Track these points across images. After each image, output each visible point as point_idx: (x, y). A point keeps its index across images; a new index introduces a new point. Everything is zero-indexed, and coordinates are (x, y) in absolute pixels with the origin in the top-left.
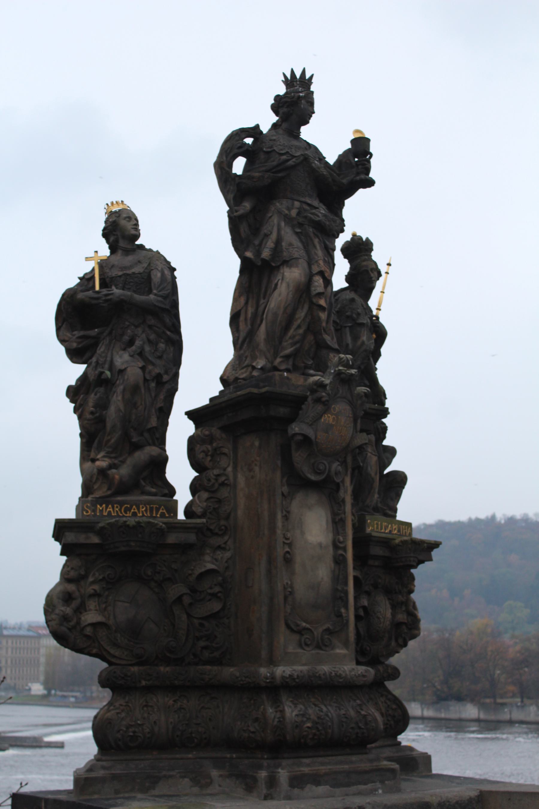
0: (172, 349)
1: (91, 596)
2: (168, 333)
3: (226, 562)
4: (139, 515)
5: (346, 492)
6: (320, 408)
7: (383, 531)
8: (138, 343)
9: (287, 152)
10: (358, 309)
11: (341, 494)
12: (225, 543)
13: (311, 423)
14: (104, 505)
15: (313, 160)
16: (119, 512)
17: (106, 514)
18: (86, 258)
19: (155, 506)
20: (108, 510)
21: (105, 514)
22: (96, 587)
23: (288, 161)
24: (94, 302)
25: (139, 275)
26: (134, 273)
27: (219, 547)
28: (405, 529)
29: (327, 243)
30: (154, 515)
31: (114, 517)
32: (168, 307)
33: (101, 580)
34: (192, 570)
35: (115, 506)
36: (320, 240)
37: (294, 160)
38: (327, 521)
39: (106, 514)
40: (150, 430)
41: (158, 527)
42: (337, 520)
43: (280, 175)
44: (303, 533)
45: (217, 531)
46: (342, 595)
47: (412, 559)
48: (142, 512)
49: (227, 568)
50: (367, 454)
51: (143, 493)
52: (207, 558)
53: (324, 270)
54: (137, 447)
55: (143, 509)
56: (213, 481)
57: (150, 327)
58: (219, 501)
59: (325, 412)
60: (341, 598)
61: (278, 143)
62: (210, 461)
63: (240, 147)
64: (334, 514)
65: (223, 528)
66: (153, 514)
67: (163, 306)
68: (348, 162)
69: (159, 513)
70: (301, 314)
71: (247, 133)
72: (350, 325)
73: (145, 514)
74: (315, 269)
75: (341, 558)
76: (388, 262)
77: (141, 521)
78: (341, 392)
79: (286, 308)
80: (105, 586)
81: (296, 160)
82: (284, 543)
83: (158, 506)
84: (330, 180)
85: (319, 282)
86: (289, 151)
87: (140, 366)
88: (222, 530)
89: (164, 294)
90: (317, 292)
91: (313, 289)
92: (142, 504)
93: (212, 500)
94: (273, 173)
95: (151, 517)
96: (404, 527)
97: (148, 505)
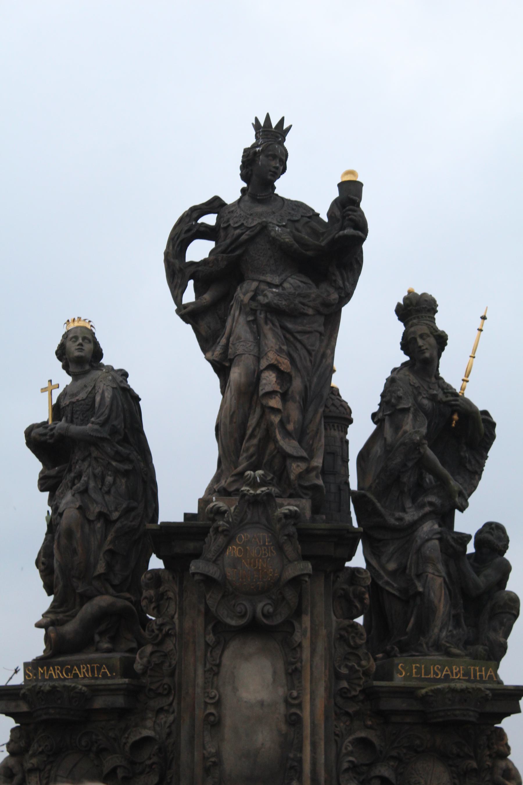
0: (123, 481)
1: (31, 771)
2: (114, 463)
3: (169, 727)
4: (80, 676)
5: (304, 634)
6: (221, 540)
7: (432, 676)
8: (84, 479)
9: (242, 224)
10: (399, 390)
11: (297, 637)
12: (171, 704)
13: (214, 558)
14: (45, 668)
15: (273, 227)
16: (60, 675)
17: (48, 678)
18: (42, 389)
19: (95, 665)
20: (50, 672)
21: (47, 677)
22: (34, 761)
23: (242, 234)
24: (43, 439)
25: (83, 402)
26: (78, 401)
27: (161, 710)
28: (480, 671)
29: (290, 326)
30: (96, 676)
31: (56, 680)
32: (105, 435)
33: (42, 753)
34: (128, 738)
35: (56, 667)
36: (273, 324)
37: (247, 233)
38: (275, 673)
39: (48, 678)
40: (99, 576)
41: (77, 690)
42: (290, 671)
43: (238, 252)
44: (235, 690)
45: (160, 690)
46: (296, 764)
47: (457, 712)
48: (84, 673)
49: (169, 734)
50: (427, 576)
51: (97, 650)
52: (149, 723)
53: (276, 363)
54: (86, 598)
55: (84, 670)
56: (156, 632)
57: (96, 459)
58: (166, 655)
59: (228, 544)
60: (292, 768)
61: (235, 215)
62: (154, 609)
63: (188, 230)
64: (288, 663)
65: (166, 686)
66: (95, 675)
67: (99, 435)
68: (333, 215)
69: (101, 673)
70: (253, 421)
71: (199, 211)
72: (388, 413)
73: (87, 675)
74: (264, 363)
75: (293, 718)
76: (482, 314)
77: (57, 685)
78: (249, 516)
79: (232, 417)
80: (45, 759)
81: (251, 232)
82: (206, 704)
83: (99, 665)
84: (296, 245)
85: (268, 379)
86: (245, 222)
87: (77, 506)
88: (166, 689)
89: (100, 420)
90: (264, 391)
91: (260, 388)
92: (82, 664)
93: (158, 654)
94: (229, 253)
95: (93, 678)
96: (477, 668)
97: (90, 664)
